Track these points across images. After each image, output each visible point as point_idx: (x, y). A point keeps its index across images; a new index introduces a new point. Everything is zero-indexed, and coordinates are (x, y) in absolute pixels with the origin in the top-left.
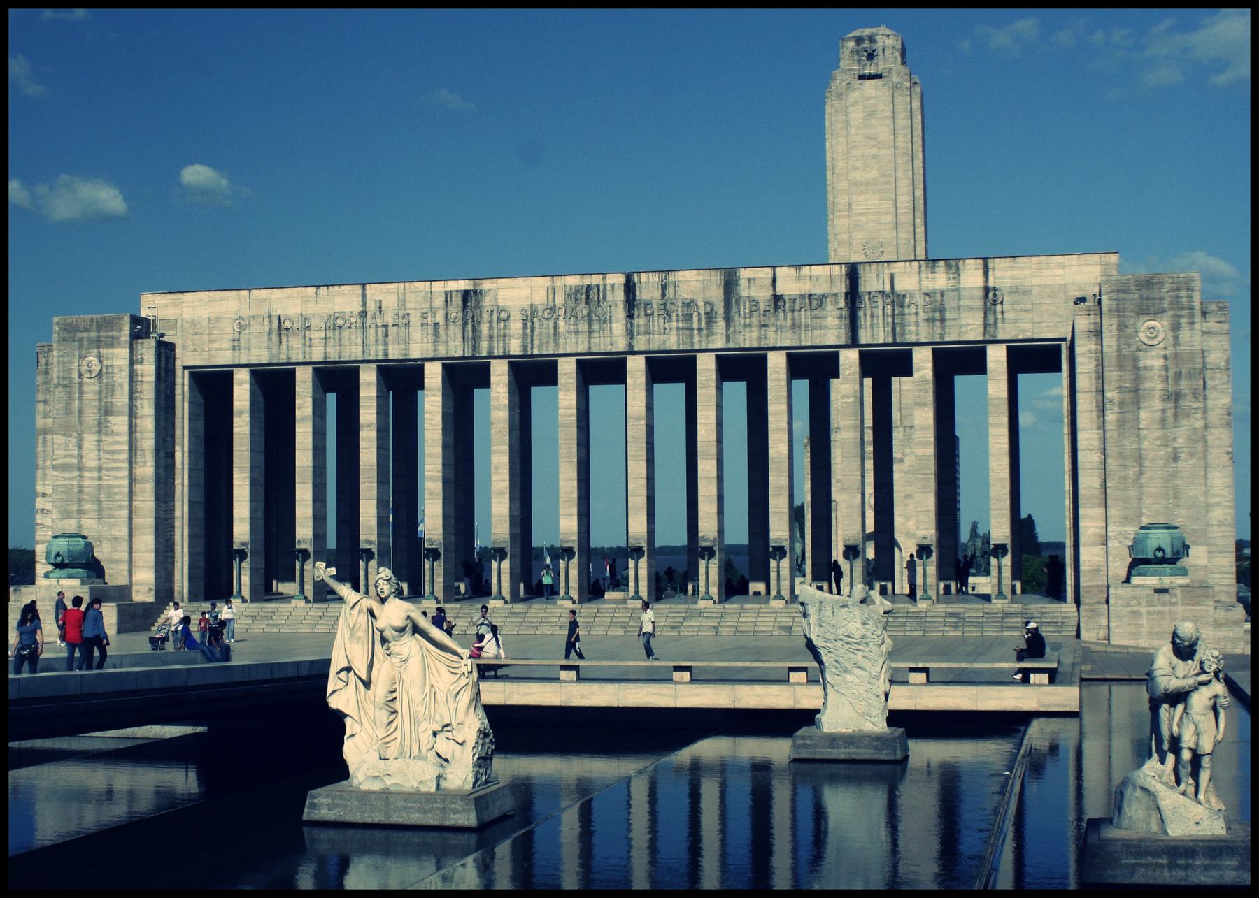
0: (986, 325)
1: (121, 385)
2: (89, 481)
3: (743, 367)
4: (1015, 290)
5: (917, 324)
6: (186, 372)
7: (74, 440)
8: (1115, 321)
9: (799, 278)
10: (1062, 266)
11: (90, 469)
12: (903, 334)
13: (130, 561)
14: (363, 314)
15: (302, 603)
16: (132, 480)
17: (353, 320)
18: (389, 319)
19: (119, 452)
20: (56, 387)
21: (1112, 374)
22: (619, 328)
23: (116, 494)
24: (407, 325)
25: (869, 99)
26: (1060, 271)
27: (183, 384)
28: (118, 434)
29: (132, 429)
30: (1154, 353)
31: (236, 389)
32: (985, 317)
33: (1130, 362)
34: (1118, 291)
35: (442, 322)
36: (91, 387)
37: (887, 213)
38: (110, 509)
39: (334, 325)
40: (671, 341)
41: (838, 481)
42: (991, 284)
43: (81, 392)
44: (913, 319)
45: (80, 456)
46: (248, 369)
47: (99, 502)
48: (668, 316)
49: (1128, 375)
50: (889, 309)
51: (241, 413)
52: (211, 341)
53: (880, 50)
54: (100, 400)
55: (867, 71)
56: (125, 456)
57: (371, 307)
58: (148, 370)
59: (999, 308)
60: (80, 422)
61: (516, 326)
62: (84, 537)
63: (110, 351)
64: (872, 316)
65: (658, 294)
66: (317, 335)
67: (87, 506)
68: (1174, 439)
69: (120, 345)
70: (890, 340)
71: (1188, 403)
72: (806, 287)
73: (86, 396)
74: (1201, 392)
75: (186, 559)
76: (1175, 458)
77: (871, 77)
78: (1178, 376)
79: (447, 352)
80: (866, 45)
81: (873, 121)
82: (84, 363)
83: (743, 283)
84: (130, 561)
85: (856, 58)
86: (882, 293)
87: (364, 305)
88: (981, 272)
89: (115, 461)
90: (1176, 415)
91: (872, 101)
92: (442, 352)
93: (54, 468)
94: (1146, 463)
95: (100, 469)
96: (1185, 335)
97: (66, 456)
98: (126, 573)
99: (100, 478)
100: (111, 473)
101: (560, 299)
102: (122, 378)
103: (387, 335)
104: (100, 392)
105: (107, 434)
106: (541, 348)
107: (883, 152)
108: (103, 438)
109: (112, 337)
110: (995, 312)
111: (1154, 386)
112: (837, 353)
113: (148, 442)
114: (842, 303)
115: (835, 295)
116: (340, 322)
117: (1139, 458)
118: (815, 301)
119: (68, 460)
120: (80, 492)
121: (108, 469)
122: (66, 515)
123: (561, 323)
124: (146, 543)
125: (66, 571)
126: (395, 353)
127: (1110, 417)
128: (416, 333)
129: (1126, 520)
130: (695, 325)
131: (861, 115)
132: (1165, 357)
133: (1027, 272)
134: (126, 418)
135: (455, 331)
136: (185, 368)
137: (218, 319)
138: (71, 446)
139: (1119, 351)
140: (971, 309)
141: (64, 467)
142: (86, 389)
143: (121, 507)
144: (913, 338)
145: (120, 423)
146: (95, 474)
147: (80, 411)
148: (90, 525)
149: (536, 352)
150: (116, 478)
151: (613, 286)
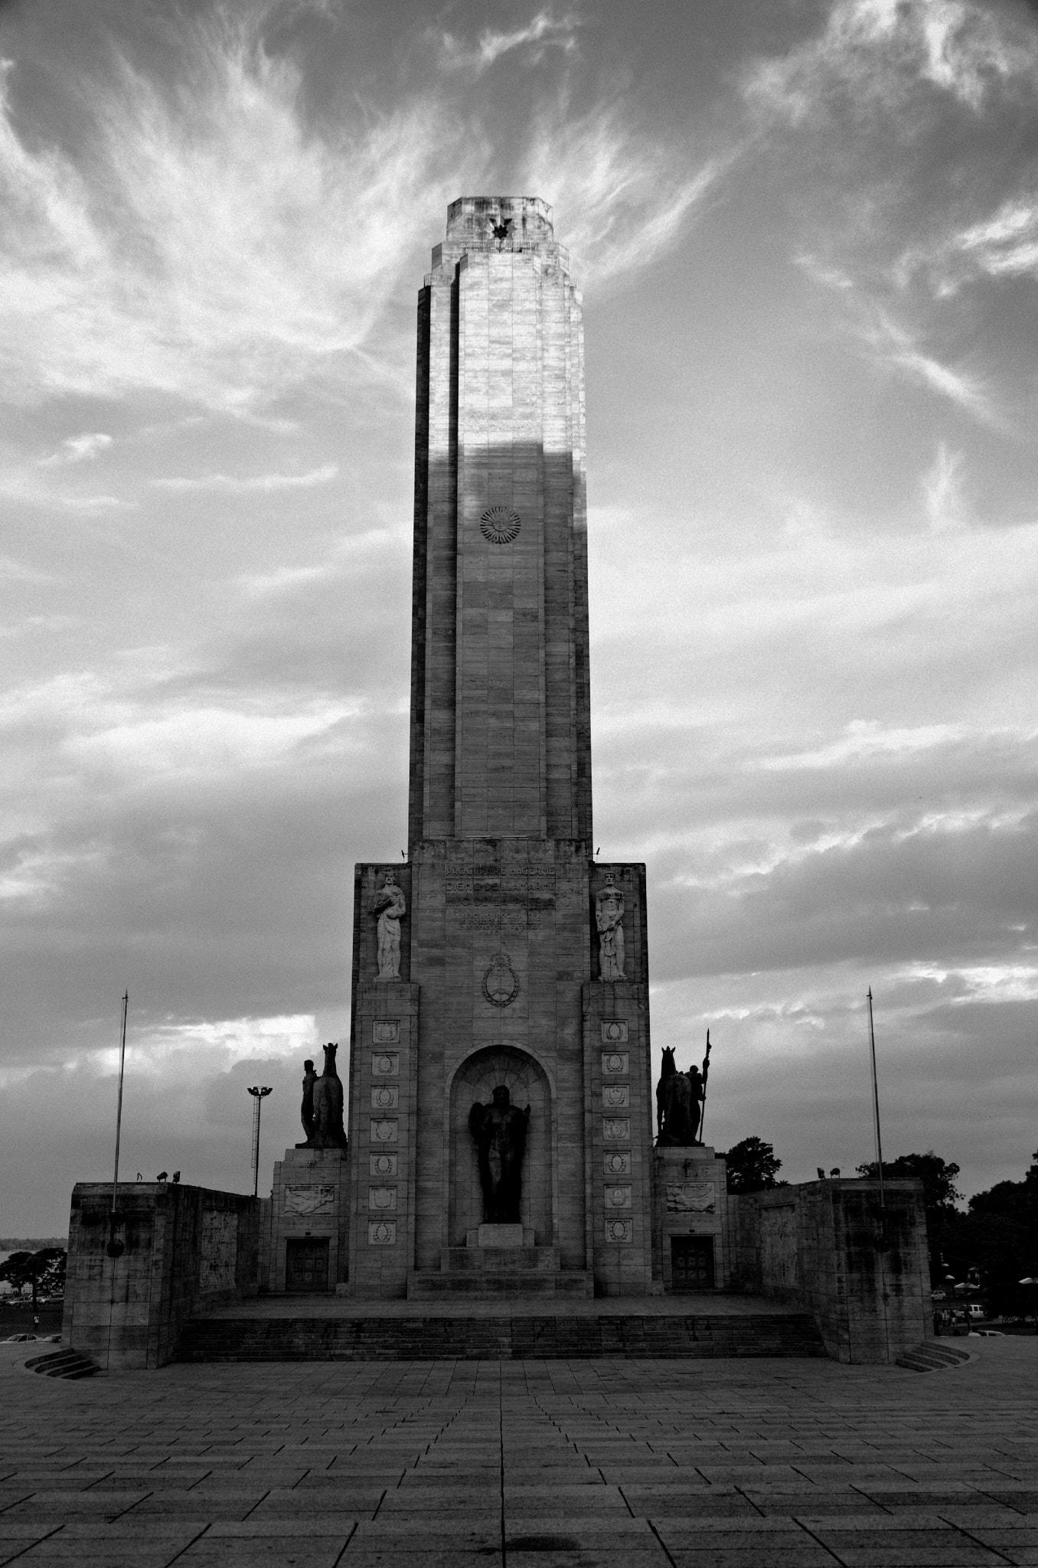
37: (527, 466)
41: (421, 944)
53: (517, 222)
81: (506, 316)
85: (477, 229)
91: (505, 285)
107: (522, 366)
131: (486, 305)
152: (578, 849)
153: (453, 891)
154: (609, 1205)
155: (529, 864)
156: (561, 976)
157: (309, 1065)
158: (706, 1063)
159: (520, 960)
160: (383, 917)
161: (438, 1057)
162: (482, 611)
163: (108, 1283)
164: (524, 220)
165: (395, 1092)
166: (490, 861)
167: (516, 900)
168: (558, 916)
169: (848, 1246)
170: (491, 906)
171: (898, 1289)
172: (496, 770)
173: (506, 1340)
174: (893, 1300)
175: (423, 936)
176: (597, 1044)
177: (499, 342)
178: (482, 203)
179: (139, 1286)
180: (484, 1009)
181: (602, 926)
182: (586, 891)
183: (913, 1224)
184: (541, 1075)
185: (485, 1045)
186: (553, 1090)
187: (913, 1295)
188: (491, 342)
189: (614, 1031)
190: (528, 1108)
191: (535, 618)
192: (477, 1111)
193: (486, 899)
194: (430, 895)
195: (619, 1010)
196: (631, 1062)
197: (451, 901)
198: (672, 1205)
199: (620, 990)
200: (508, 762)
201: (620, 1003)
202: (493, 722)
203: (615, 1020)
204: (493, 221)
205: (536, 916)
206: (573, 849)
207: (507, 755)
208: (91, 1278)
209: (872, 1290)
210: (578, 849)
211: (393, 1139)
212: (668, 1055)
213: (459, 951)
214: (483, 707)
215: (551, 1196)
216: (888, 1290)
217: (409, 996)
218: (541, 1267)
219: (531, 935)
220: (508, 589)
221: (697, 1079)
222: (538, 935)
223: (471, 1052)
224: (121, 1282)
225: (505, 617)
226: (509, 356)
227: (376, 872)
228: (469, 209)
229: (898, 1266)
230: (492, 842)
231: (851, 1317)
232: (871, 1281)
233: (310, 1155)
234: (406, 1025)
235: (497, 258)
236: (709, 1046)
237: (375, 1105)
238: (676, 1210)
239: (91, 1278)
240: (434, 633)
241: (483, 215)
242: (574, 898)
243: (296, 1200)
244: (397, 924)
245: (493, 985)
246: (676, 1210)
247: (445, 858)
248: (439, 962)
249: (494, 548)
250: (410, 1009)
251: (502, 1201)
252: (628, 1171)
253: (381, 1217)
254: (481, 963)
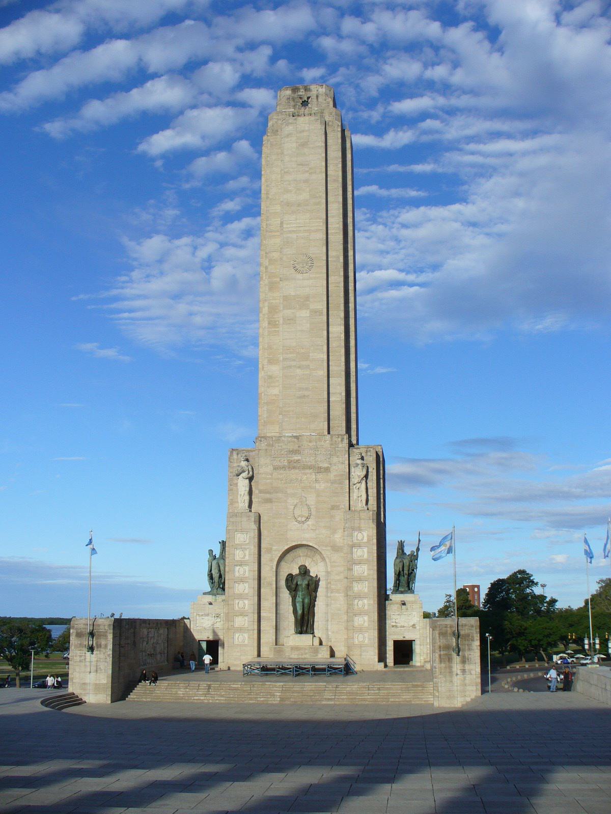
25: (303, 131)
37: (317, 231)
41: (261, 492)
80: (301, 92)
85: (292, 103)
91: (305, 134)
131: (294, 145)
152: (342, 440)
153: (276, 463)
154: (356, 624)
155: (316, 448)
156: (334, 508)
157: (211, 551)
158: (418, 549)
159: (311, 500)
161: (269, 550)
162: (293, 311)
163: (88, 664)
164: (317, 97)
165: (247, 568)
166: (296, 447)
167: (310, 467)
168: (331, 476)
169: (440, 651)
170: (297, 471)
171: (464, 671)
172: (300, 397)
173: (278, 694)
174: (460, 677)
175: (261, 488)
176: (351, 543)
177: (302, 165)
179: (102, 666)
180: (294, 525)
181: (355, 480)
182: (347, 462)
183: (473, 640)
184: (323, 559)
185: (294, 544)
186: (329, 567)
187: (471, 674)
188: (299, 165)
189: (360, 536)
190: (317, 576)
191: (321, 314)
192: (290, 578)
193: (294, 468)
194: (264, 467)
195: (362, 525)
196: (368, 552)
197: (275, 468)
198: (394, 624)
199: (363, 515)
200: (306, 393)
201: (362, 521)
202: (299, 371)
203: (360, 530)
204: (301, 98)
205: (320, 476)
206: (340, 439)
207: (307, 389)
208: (80, 661)
209: (451, 672)
210: (342, 440)
211: (246, 591)
212: (401, 545)
213: (280, 495)
214: (293, 363)
215: (328, 621)
216: (459, 672)
217: (253, 519)
218: (320, 656)
219: (317, 486)
220: (307, 298)
221: (414, 557)
222: (321, 486)
223: (286, 548)
224: (94, 663)
225: (305, 313)
226: (308, 171)
227: (238, 454)
229: (464, 661)
230: (297, 437)
231: (440, 685)
232: (450, 667)
233: (210, 598)
234: (252, 535)
235: (301, 119)
236: (419, 541)
237: (237, 574)
238: (396, 627)
239: (80, 661)
240: (269, 323)
241: (296, 95)
242: (340, 466)
243: (202, 621)
244: (247, 481)
245: (298, 512)
246: (396, 627)
247: (273, 446)
248: (269, 501)
249: (299, 276)
250: (254, 527)
251: (305, 624)
252: (366, 607)
253: (241, 630)
254: (292, 501)
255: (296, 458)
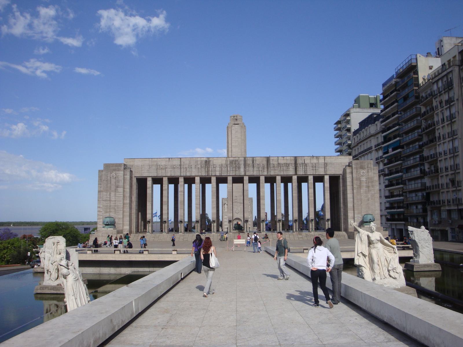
0: (325, 171)
1: (121, 180)
2: (112, 204)
3: (271, 180)
4: (331, 163)
5: (310, 171)
6: (135, 178)
7: (108, 194)
8: (356, 170)
9: (284, 160)
10: (340, 158)
11: (113, 201)
12: (307, 173)
13: (123, 224)
14: (181, 165)
15: (165, 234)
16: (124, 204)
17: (178, 166)
18: (187, 166)
19: (121, 197)
20: (104, 180)
21: (355, 182)
22: (242, 170)
23: (120, 207)
24: (191, 168)
26: (340, 160)
27: (134, 181)
28: (120, 192)
29: (124, 191)
30: (364, 177)
31: (148, 182)
32: (325, 169)
33: (359, 179)
34: (356, 164)
35: (200, 167)
36: (113, 181)
38: (118, 211)
39: (173, 167)
40: (255, 173)
42: (326, 162)
43: (110, 182)
44: (309, 169)
45: (110, 198)
46: (151, 178)
47: (115, 209)
48: (253, 167)
49: (359, 182)
50: (304, 167)
51: (149, 188)
52: (142, 170)
53: (238, 119)
54: (116, 184)
55: (236, 123)
56: (122, 198)
57: (182, 163)
58: (128, 177)
59: (327, 167)
60: (110, 190)
61: (218, 169)
62: (113, 218)
63: (118, 172)
64: (300, 168)
65: (251, 162)
66: (168, 170)
67: (112, 210)
68: (368, 196)
69: (121, 171)
70: (304, 174)
71: (371, 188)
72: (285, 162)
73: (112, 183)
74: (373, 186)
75: (135, 223)
76: (368, 200)
77: (236, 124)
78: (369, 182)
79: (201, 174)
82: (112, 175)
83: (271, 160)
84: (123, 224)
85: (233, 120)
86: (302, 164)
87: (181, 163)
88: (323, 159)
89: (120, 199)
90: (368, 191)
91: (237, 129)
92: (200, 174)
93: (103, 200)
94: (362, 201)
95: (115, 201)
96: (370, 174)
97: (106, 198)
98: (122, 227)
99: (115, 203)
100: (118, 202)
101: (228, 163)
102: (121, 178)
103: (186, 170)
104: (116, 182)
105: (117, 192)
106: (224, 174)
108: (116, 193)
109: (119, 169)
110: (327, 168)
111: (364, 184)
112: (292, 176)
113: (128, 195)
114: (293, 165)
115: (292, 163)
116: (174, 167)
117: (361, 200)
118: (287, 165)
119: (107, 199)
120: (110, 206)
121: (117, 201)
122: (106, 212)
123: (229, 168)
124: (127, 219)
125: (109, 226)
126: (188, 174)
127: (355, 191)
128: (194, 170)
129: (359, 213)
130: (260, 169)
132: (366, 178)
133: (333, 160)
134: (122, 189)
135: (203, 169)
136: (135, 177)
137: (144, 165)
138: (108, 195)
139: (356, 177)
140: (321, 167)
141: (106, 200)
142: (112, 181)
143: (121, 211)
144: (309, 174)
145: (121, 190)
146: (114, 202)
147: (110, 187)
148: (112, 215)
149: (223, 175)
150: (120, 203)
151: (241, 160)
160: (225, 205)
178: (234, 117)
205: (241, 204)
228: (233, 117)
255: (236, 201)
